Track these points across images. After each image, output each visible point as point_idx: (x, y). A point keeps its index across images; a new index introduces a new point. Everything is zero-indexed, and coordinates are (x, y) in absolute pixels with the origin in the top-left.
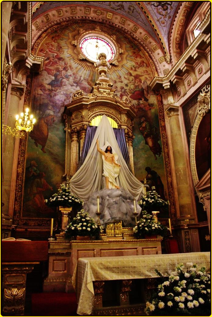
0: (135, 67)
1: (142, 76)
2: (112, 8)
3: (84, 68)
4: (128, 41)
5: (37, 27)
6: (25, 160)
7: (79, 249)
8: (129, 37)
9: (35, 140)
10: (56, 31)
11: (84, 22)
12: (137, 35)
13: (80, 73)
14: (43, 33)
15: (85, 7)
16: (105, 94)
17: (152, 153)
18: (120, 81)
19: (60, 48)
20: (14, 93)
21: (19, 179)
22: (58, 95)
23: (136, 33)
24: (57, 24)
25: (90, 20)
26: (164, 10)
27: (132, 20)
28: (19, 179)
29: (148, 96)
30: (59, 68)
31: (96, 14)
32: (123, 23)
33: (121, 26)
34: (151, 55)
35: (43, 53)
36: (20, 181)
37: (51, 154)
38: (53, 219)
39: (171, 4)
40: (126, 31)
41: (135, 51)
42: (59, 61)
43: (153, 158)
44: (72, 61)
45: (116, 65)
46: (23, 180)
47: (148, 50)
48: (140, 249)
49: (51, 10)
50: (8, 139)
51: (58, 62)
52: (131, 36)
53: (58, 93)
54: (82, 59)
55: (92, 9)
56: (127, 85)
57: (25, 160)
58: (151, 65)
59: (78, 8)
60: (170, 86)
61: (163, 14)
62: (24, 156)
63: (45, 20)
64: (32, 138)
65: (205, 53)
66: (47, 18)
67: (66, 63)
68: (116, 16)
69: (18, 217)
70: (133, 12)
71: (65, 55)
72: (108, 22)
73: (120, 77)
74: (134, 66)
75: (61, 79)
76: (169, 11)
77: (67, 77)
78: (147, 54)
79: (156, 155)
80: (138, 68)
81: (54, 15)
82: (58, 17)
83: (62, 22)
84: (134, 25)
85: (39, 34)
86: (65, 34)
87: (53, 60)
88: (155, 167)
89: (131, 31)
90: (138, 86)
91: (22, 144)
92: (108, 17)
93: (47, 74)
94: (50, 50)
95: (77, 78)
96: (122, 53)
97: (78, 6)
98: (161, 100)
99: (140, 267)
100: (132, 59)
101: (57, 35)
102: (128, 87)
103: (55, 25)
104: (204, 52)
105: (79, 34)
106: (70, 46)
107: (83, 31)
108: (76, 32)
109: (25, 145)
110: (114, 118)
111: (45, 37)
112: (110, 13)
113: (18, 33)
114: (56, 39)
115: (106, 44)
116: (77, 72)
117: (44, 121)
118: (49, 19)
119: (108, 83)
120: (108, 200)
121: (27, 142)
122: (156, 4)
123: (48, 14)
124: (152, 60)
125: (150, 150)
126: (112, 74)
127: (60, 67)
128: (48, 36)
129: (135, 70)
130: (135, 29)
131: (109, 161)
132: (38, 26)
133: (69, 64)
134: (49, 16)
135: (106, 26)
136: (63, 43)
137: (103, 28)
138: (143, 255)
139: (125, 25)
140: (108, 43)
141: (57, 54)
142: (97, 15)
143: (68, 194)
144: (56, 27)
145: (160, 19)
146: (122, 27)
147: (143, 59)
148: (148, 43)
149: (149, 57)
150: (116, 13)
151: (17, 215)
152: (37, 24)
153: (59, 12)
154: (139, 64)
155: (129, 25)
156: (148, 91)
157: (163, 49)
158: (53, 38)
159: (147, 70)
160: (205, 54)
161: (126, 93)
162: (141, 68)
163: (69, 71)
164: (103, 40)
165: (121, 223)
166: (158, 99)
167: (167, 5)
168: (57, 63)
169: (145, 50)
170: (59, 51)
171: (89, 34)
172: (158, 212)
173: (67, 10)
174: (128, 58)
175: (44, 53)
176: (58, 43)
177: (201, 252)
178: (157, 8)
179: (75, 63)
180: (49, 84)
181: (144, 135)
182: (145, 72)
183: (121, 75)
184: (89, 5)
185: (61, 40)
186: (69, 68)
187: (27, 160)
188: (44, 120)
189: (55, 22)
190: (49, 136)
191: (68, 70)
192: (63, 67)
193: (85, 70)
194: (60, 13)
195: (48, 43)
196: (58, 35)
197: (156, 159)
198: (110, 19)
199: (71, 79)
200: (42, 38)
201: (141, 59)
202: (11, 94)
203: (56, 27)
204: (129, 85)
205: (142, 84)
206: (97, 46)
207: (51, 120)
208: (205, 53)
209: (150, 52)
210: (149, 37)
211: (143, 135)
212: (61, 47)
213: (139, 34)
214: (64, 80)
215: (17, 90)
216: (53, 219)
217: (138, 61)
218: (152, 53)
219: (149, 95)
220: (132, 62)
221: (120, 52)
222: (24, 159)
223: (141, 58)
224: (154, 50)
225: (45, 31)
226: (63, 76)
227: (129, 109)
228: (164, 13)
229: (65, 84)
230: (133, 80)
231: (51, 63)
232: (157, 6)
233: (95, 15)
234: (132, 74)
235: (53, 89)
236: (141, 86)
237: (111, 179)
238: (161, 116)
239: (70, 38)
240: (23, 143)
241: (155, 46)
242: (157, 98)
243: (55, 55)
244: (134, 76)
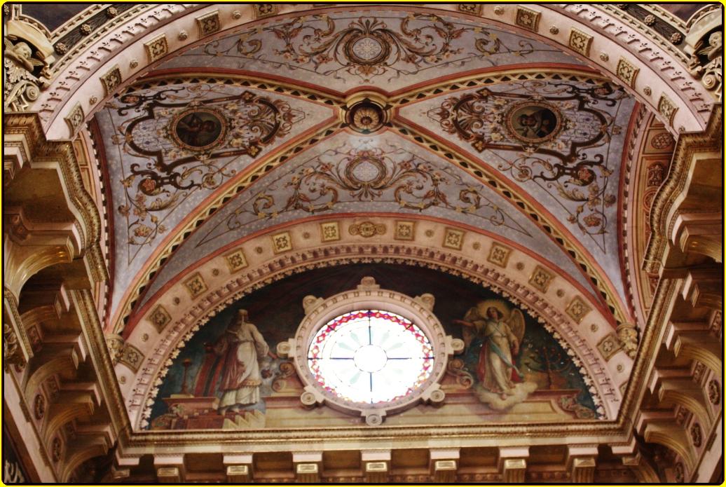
26: (585, 184)
39: (602, 161)
61: (586, 197)
65: (709, 331)
70: (478, 206)
76: (599, 182)
81: (216, 272)
104: (706, 328)
122: (548, 175)
145: (578, 213)
157: (608, 312)
160: (712, 334)
167: (589, 167)
178: (555, 182)
208: (709, 331)
228: (585, 191)
232: (556, 178)
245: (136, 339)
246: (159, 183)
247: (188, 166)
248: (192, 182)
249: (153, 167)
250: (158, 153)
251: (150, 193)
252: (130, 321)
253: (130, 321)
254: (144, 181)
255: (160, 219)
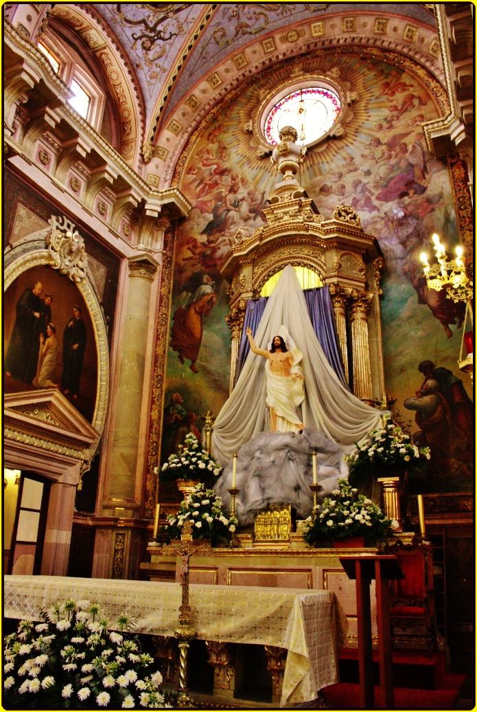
0: (388, 119)
1: (407, 134)
2: (314, 11)
3: (269, 172)
4: (371, 63)
5: (176, 130)
6: (164, 393)
7: (327, 568)
8: (375, 52)
9: (179, 352)
10: (215, 119)
11: (270, 70)
12: (390, 39)
13: (262, 187)
14: (192, 134)
15: (261, 42)
16: (286, 218)
17: (438, 321)
18: (352, 168)
19: (223, 149)
20: (136, 272)
21: (154, 432)
22: (219, 248)
23: (385, 34)
24: (217, 103)
25: (281, 62)
27: (369, 11)
28: (154, 432)
29: (425, 178)
30: (222, 192)
31: (289, 42)
32: (351, 27)
33: (350, 37)
34: (432, 69)
35: (193, 174)
36: (155, 436)
37: (207, 372)
38: (420, 497)
40: (364, 41)
41: (388, 80)
42: (221, 178)
43: (443, 334)
44: (246, 168)
45: (339, 135)
46: (159, 434)
47: (423, 60)
48: (317, 571)
49: (194, 86)
50: (126, 361)
51: (219, 182)
52: (378, 48)
53: (219, 244)
54: (263, 154)
55: (277, 37)
56: (368, 173)
57: (164, 393)
58: (433, 97)
59: (248, 51)
60: (467, 133)
62: (160, 387)
63: (188, 109)
64: (174, 350)
66: (193, 103)
67: (235, 176)
68: (331, 23)
69: (152, 503)
71: (231, 162)
72: (319, 45)
73: (352, 159)
74: (385, 119)
75: (225, 213)
77: (236, 205)
78: (421, 72)
79: (451, 326)
80: (398, 118)
81: (204, 91)
82: (214, 89)
83: (225, 95)
84: (376, 19)
85: (183, 141)
86: (232, 116)
87: (210, 180)
88: (446, 358)
89: (376, 37)
90: (398, 163)
91: (158, 364)
92: (315, 35)
93: (200, 213)
94: (205, 162)
95: (256, 200)
96: (353, 102)
97: (248, 47)
98: (463, 176)
99: (209, 613)
100: (383, 102)
101: (217, 125)
102: (372, 176)
103: (213, 108)
105: (259, 102)
106: (242, 137)
107: (264, 92)
108: (254, 101)
109: (163, 365)
110: (312, 266)
111: (195, 141)
112: (315, 24)
113: (95, 171)
114: (215, 136)
115: (322, 95)
116: (255, 187)
117: (196, 311)
118: (196, 103)
119: (294, 189)
120: (259, 458)
121: (166, 359)
123: (193, 95)
124: (438, 81)
125: (433, 317)
126: (332, 160)
127: (223, 190)
128: (201, 137)
129: (391, 127)
130: (381, 27)
131: (277, 370)
132: (178, 127)
133: (240, 177)
134: (195, 99)
135: (317, 56)
136: (227, 138)
137: (310, 63)
138: (310, 590)
139: (359, 30)
140: (325, 91)
141: (217, 164)
142: (292, 42)
143: (194, 453)
144: (214, 111)
146: (354, 39)
147: (411, 89)
148: (417, 43)
149: (426, 78)
150: (329, 16)
151: (150, 499)
152: (174, 124)
153: (211, 80)
154: (399, 108)
155: (365, 25)
156: (425, 168)
158: (210, 134)
159: (422, 112)
161: (367, 193)
162: (404, 115)
163: (240, 191)
164: (315, 89)
165: (288, 509)
166: (453, 177)
168: (218, 184)
169: (416, 63)
170: (221, 156)
171: (278, 92)
172: (397, 479)
173: (228, 67)
174: (370, 106)
175: (195, 172)
176: (219, 142)
177: (128, 579)
179: (253, 169)
180: (203, 233)
181: (415, 281)
182: (416, 121)
183: (353, 155)
184: (269, 33)
185: (225, 132)
186: (240, 184)
187: (166, 394)
188: (195, 309)
189: (211, 103)
190: (203, 338)
191: (237, 190)
192: (229, 188)
193: (272, 175)
194: (214, 80)
195: (202, 150)
196: (219, 126)
197: (450, 334)
198: (320, 36)
199: (245, 208)
200: (189, 146)
201: (406, 93)
202: (130, 276)
203: (214, 111)
204: (374, 171)
205: (407, 155)
206: (301, 111)
207: (207, 305)
209: (428, 64)
210: (417, 28)
211: (412, 282)
212: (224, 148)
213: (393, 33)
214: (232, 213)
215: (140, 266)
216: (420, 497)
217: (398, 100)
218: (433, 65)
219: (427, 176)
220: (382, 109)
221: (349, 101)
222: (162, 392)
223: (405, 90)
224: (434, 54)
225: (196, 129)
226: (228, 206)
227: (335, 235)
229: (233, 221)
230: (384, 153)
231: (207, 187)
233: (289, 45)
234: (382, 141)
235: (211, 238)
236: (407, 160)
237: (282, 409)
238: (464, 217)
239: (242, 120)
240: (159, 362)
241: (433, 43)
242: (453, 173)
243: (213, 169)
244: (385, 144)
245: (162, 142)
246: (152, 41)
247: (165, 23)
248: (171, 33)
249: (144, 31)
250: (143, 21)
251: (149, 49)
252: (158, 130)
253: (158, 130)
254: (143, 43)
255: (161, 64)
